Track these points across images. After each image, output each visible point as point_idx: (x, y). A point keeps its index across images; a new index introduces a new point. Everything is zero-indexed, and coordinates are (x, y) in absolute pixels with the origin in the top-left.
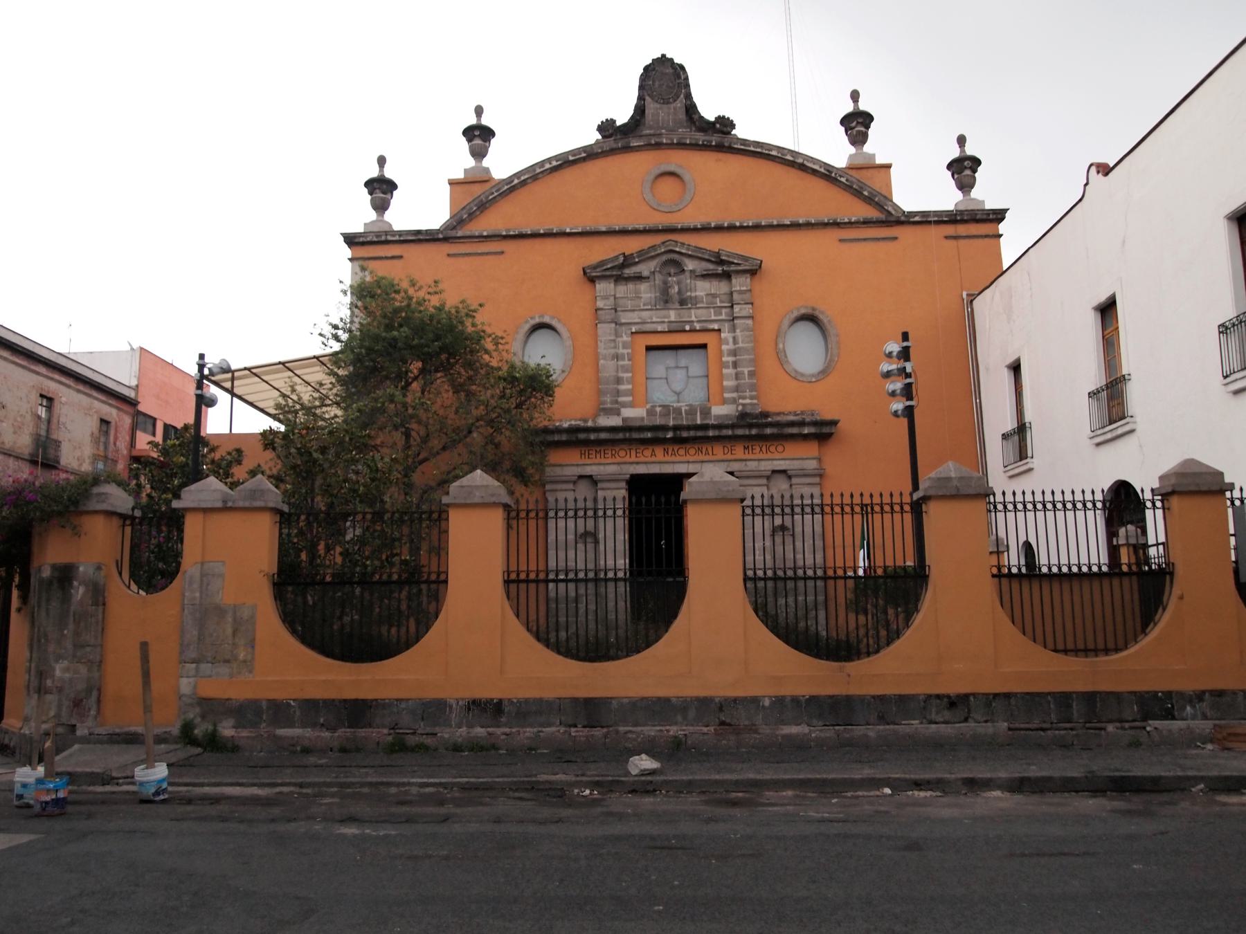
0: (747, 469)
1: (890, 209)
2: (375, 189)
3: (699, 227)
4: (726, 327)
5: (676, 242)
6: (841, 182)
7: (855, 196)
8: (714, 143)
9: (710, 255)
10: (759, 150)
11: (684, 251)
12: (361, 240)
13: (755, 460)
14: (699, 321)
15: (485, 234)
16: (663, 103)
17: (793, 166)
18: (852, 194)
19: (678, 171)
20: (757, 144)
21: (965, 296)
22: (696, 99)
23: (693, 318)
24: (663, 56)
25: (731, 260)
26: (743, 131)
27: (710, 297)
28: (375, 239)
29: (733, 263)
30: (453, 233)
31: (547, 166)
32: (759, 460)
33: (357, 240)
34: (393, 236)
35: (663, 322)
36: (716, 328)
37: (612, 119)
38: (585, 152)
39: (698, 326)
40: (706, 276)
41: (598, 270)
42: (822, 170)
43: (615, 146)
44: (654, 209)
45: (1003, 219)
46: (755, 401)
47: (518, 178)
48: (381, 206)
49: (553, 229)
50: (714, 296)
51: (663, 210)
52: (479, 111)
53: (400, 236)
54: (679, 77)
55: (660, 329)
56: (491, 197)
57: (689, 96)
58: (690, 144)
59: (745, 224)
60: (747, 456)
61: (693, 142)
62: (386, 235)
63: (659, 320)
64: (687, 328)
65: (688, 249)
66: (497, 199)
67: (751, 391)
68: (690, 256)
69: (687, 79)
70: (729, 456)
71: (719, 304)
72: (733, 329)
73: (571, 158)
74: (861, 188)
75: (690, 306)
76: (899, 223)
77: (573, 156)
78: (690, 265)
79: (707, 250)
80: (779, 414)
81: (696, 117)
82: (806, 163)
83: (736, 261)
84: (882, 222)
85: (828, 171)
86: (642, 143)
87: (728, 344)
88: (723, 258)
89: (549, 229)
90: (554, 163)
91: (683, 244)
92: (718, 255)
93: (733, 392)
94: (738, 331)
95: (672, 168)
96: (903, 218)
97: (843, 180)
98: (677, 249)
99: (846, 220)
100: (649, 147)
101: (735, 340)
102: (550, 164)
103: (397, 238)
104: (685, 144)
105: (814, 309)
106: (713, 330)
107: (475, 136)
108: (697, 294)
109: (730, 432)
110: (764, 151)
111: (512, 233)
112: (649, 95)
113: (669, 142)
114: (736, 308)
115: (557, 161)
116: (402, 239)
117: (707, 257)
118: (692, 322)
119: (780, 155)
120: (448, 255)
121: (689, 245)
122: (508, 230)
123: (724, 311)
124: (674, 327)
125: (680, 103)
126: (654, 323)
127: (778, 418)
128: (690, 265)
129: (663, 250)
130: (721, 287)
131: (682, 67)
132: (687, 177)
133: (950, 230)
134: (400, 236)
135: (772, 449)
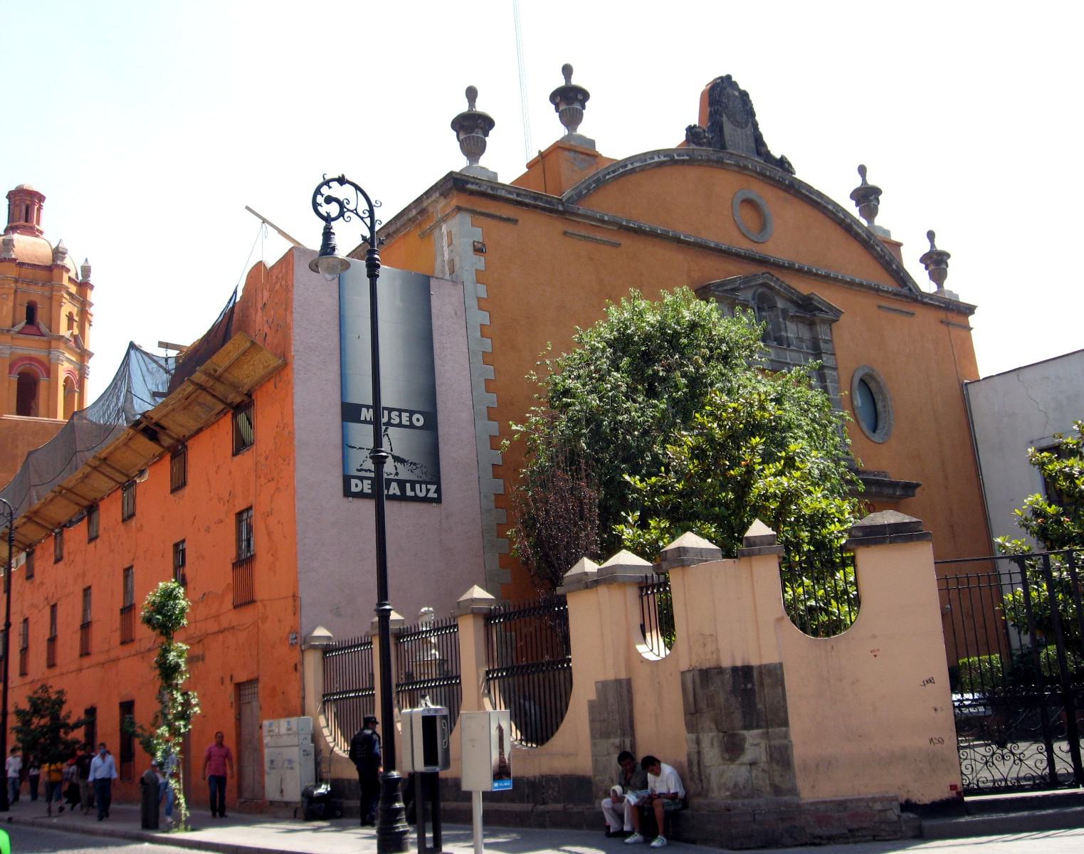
2: (477, 127)
5: (773, 276)
6: (876, 250)
8: (787, 182)
10: (820, 200)
17: (840, 224)
18: (881, 264)
19: (759, 201)
23: (789, 361)
24: (729, 77)
25: (820, 306)
26: (801, 174)
28: (489, 191)
29: (822, 310)
31: (656, 159)
33: (469, 186)
34: (510, 193)
37: (687, 129)
38: (687, 155)
41: (720, 289)
47: (632, 164)
50: (801, 340)
52: (567, 71)
53: (518, 195)
56: (607, 177)
57: (755, 125)
65: (781, 286)
73: (676, 158)
76: (915, 300)
79: (796, 291)
81: (763, 150)
82: (853, 224)
83: (824, 309)
84: (906, 297)
85: (868, 237)
86: (733, 163)
88: (815, 303)
89: (665, 231)
90: (663, 159)
91: (778, 279)
94: (828, 381)
95: (753, 196)
97: (879, 249)
99: (885, 289)
102: (659, 157)
103: (514, 197)
107: (577, 99)
108: (789, 335)
110: (823, 203)
111: (631, 225)
113: (754, 169)
116: (519, 199)
119: (834, 210)
121: (783, 282)
122: (628, 221)
125: (749, 130)
128: (780, 304)
129: (761, 281)
130: (805, 333)
131: (744, 95)
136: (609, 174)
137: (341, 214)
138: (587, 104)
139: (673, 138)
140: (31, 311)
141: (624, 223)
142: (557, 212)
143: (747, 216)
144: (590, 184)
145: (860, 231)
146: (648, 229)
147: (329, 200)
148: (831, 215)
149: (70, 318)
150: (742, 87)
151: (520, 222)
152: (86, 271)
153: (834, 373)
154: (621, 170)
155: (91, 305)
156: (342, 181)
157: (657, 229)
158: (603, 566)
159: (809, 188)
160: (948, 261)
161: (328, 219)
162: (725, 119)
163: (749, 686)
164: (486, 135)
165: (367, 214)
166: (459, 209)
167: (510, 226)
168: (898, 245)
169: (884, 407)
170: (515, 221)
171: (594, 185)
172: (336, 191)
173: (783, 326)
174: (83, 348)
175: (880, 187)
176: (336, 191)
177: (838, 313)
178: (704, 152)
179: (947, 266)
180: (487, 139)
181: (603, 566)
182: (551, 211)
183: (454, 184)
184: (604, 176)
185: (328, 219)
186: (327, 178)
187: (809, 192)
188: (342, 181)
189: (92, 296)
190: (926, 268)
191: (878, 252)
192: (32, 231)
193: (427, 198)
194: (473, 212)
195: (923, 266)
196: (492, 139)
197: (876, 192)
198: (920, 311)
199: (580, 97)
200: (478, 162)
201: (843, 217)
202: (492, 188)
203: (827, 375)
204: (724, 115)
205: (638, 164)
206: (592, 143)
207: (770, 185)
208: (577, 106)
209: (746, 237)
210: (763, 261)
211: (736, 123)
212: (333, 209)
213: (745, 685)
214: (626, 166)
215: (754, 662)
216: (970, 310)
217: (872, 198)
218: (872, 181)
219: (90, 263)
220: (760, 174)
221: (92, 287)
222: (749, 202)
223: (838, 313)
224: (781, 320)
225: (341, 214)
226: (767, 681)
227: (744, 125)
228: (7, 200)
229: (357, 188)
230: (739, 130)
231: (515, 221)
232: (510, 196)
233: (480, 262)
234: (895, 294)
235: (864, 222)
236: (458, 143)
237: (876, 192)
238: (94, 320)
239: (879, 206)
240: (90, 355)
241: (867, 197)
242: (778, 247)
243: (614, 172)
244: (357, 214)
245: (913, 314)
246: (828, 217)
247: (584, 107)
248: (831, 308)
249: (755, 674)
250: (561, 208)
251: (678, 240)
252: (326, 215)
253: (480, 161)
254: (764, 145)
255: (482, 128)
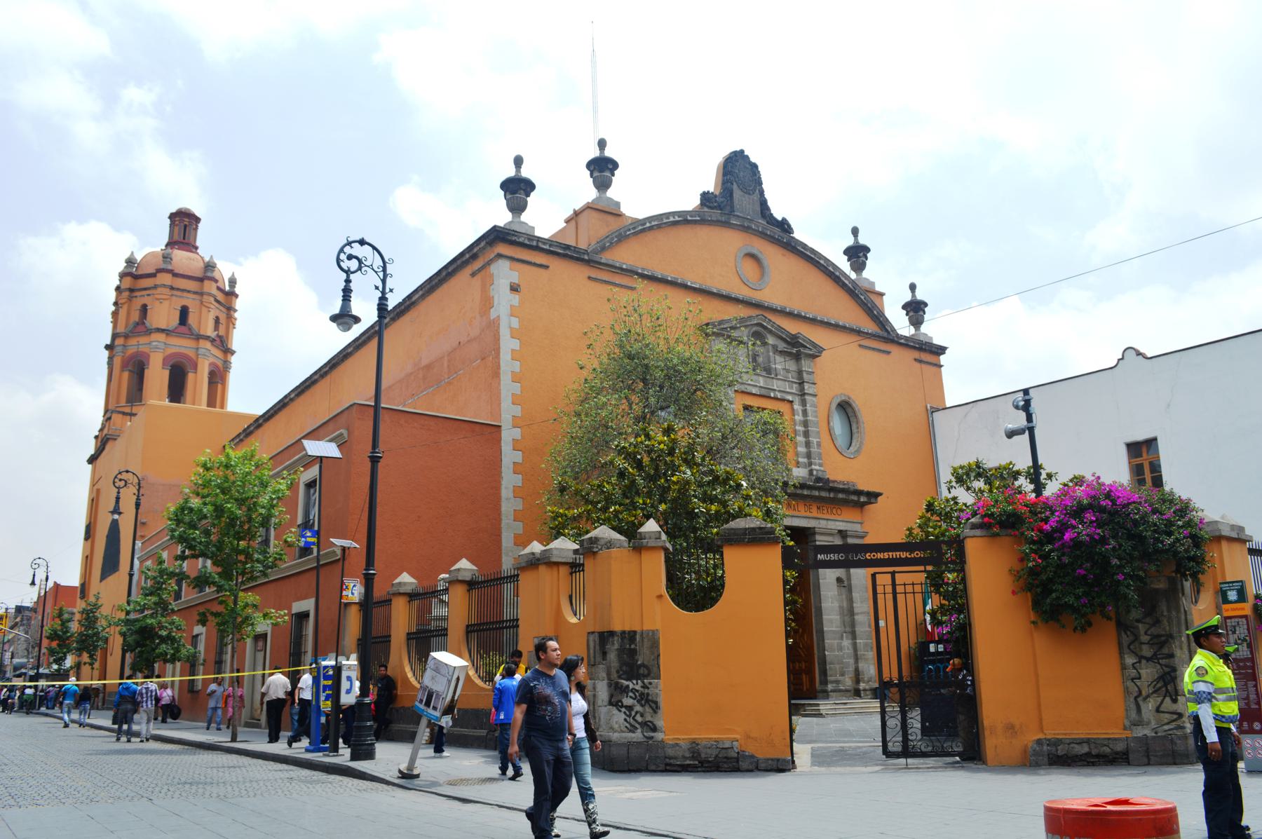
0: (821, 527)
1: (889, 329)
2: (521, 189)
3: (779, 309)
4: (797, 400)
5: (766, 318)
7: (866, 312)
9: (787, 335)
11: (769, 327)
12: (514, 238)
13: (824, 519)
14: (780, 391)
15: (624, 267)
16: (746, 193)
17: (830, 277)
19: (760, 255)
20: (813, 251)
21: (929, 408)
22: (767, 195)
23: (775, 388)
24: (742, 151)
26: (799, 234)
27: (785, 371)
28: (527, 242)
29: (806, 347)
30: (597, 258)
31: (672, 219)
32: (828, 520)
34: (544, 243)
35: (756, 386)
36: (791, 399)
37: (701, 195)
38: (699, 217)
39: (779, 395)
40: (782, 353)
42: (850, 285)
43: (720, 218)
44: (744, 283)
45: (944, 353)
46: (822, 469)
47: (650, 222)
48: (517, 207)
49: (678, 279)
50: (788, 371)
51: (751, 286)
53: (550, 246)
54: (756, 175)
55: (754, 391)
56: (628, 233)
57: (762, 192)
58: (770, 236)
59: (808, 316)
60: (820, 516)
61: (772, 234)
62: (538, 241)
63: (752, 383)
64: (772, 395)
65: (772, 326)
66: (631, 236)
67: (819, 459)
68: (770, 332)
69: (760, 178)
70: (808, 514)
71: (791, 380)
72: (804, 403)
73: (689, 218)
74: (873, 307)
75: (773, 376)
77: (691, 216)
78: (771, 340)
80: (834, 482)
84: (884, 338)
87: (799, 415)
88: (800, 341)
89: (674, 278)
90: (677, 219)
92: (795, 337)
93: (804, 458)
94: (808, 405)
95: (755, 252)
96: (896, 339)
97: (862, 297)
98: (765, 324)
99: (866, 331)
100: (740, 228)
101: (805, 413)
102: (674, 218)
103: (547, 247)
104: (767, 234)
105: (849, 398)
106: (789, 401)
109: (816, 493)
111: (646, 273)
112: (736, 181)
114: (806, 386)
115: (679, 217)
116: (551, 249)
117: (784, 336)
118: (775, 390)
119: (825, 265)
120: (589, 278)
121: (774, 323)
122: (643, 269)
123: (795, 386)
124: (764, 392)
125: (756, 197)
126: (749, 385)
127: (836, 485)
128: (771, 340)
129: (755, 322)
130: (792, 365)
131: (755, 166)
132: (765, 263)
133: (916, 354)
134: (550, 246)
135: (834, 511)
136: (629, 230)
137: (360, 269)
138: (616, 172)
139: (690, 202)
140: (184, 312)
141: (640, 271)
142: (582, 260)
143: (749, 268)
144: (613, 239)
145: (847, 282)
146: (660, 276)
147: (350, 257)
148: (822, 268)
149: (217, 320)
150: (753, 160)
151: (551, 267)
152: (233, 282)
153: (814, 399)
154: (640, 228)
155: (235, 311)
156: (362, 242)
157: (668, 276)
158: (548, 547)
159: (804, 246)
160: (926, 309)
161: (348, 272)
162: (735, 186)
163: (633, 646)
164: (528, 195)
165: (381, 269)
166: (500, 256)
167: (541, 271)
168: (882, 295)
169: (858, 428)
170: (547, 267)
171: (616, 239)
172: (357, 250)
173: (772, 359)
174: (227, 346)
175: (868, 246)
176: (357, 250)
177: (820, 350)
178: (716, 214)
179: (924, 313)
180: (528, 199)
181: (548, 547)
182: (578, 259)
183: (496, 236)
184: (626, 232)
185: (348, 272)
186: (350, 240)
187: (804, 249)
188: (362, 242)
189: (239, 304)
190: (907, 315)
191: (862, 300)
192: (191, 247)
193: (477, 245)
194: (512, 259)
195: (905, 312)
196: (532, 200)
197: (866, 249)
198: (895, 350)
199: (611, 167)
200: (520, 217)
201: (832, 270)
202: (529, 239)
203: (808, 401)
204: (734, 183)
205: (656, 223)
206: (618, 204)
207: (771, 242)
208: (607, 174)
209: (746, 284)
210: (758, 306)
211: (746, 191)
212: (353, 265)
213: (630, 646)
214: (645, 224)
215: (637, 628)
216: (941, 350)
217: (861, 254)
218: (862, 240)
219: (236, 276)
220: (760, 232)
221: (237, 296)
222: (752, 256)
223: (820, 350)
224: (771, 354)
225: (360, 269)
226: (646, 644)
227: (751, 192)
228: (169, 220)
229: (374, 248)
230: (747, 196)
231: (547, 267)
232: (545, 247)
233: (515, 299)
234: (874, 336)
235: (853, 276)
236: (505, 201)
237: (866, 249)
238: (238, 323)
239: (867, 262)
240: (233, 353)
241: (857, 254)
242: (772, 295)
243: (634, 228)
244: (373, 269)
245: (889, 353)
246: (820, 269)
247: (613, 175)
248: (815, 345)
249: (638, 637)
250: (586, 257)
251: (684, 287)
252: (347, 269)
253: (522, 217)
254: (768, 209)
255: (524, 190)
